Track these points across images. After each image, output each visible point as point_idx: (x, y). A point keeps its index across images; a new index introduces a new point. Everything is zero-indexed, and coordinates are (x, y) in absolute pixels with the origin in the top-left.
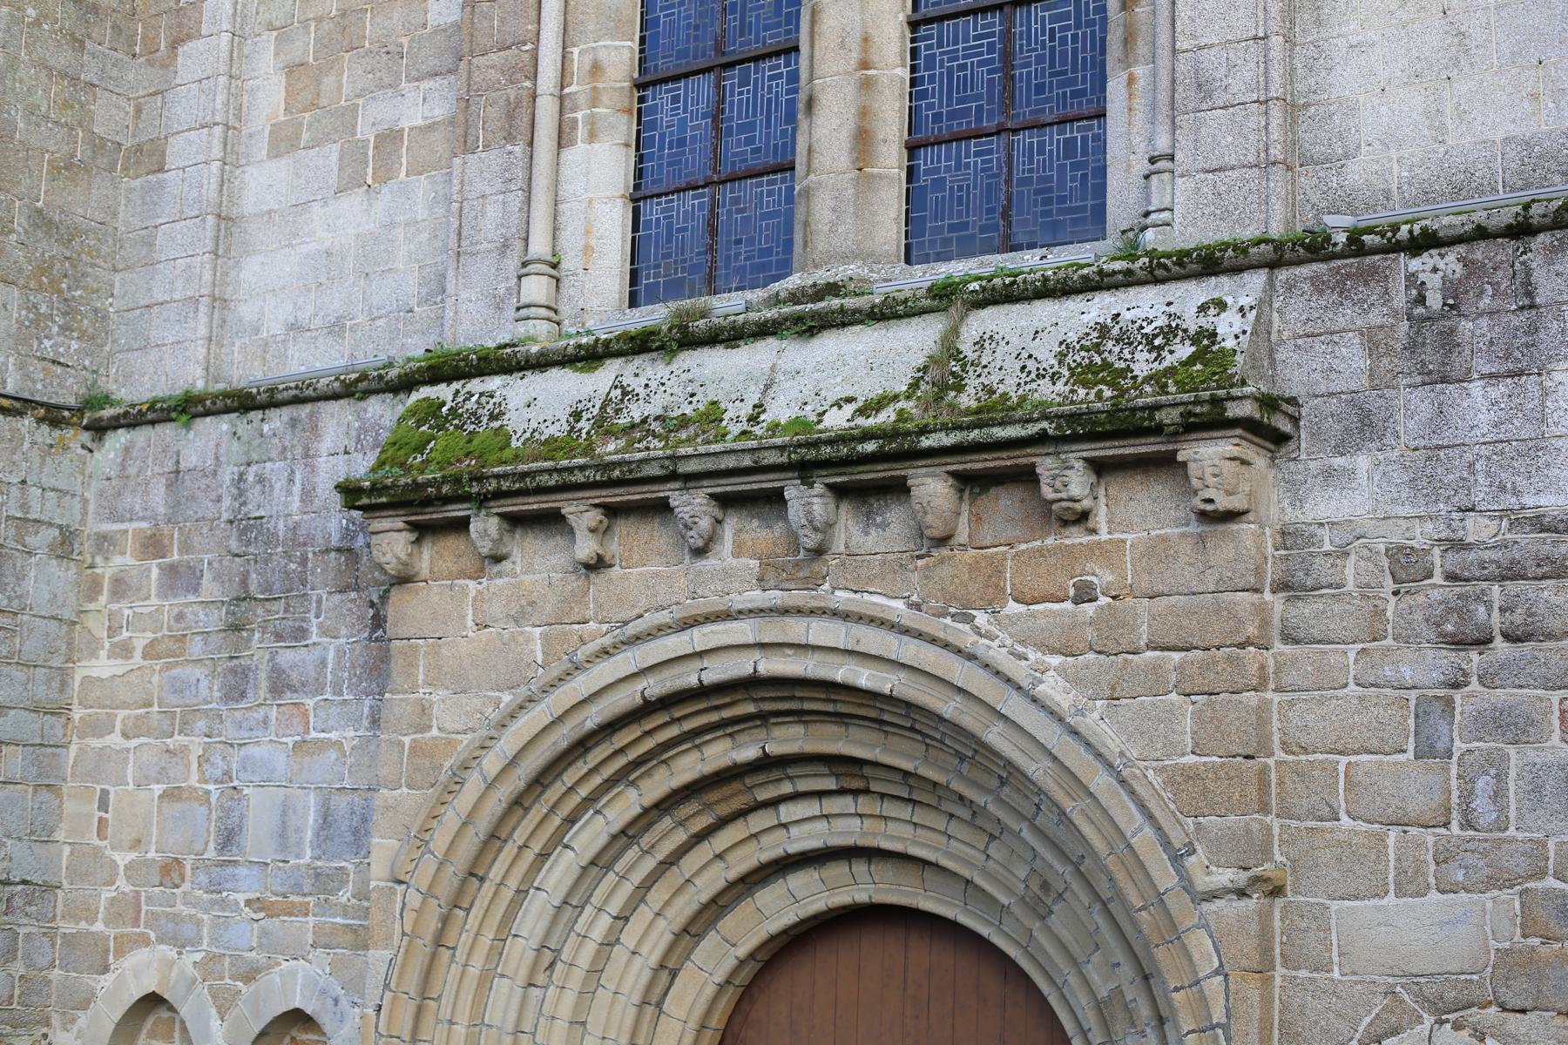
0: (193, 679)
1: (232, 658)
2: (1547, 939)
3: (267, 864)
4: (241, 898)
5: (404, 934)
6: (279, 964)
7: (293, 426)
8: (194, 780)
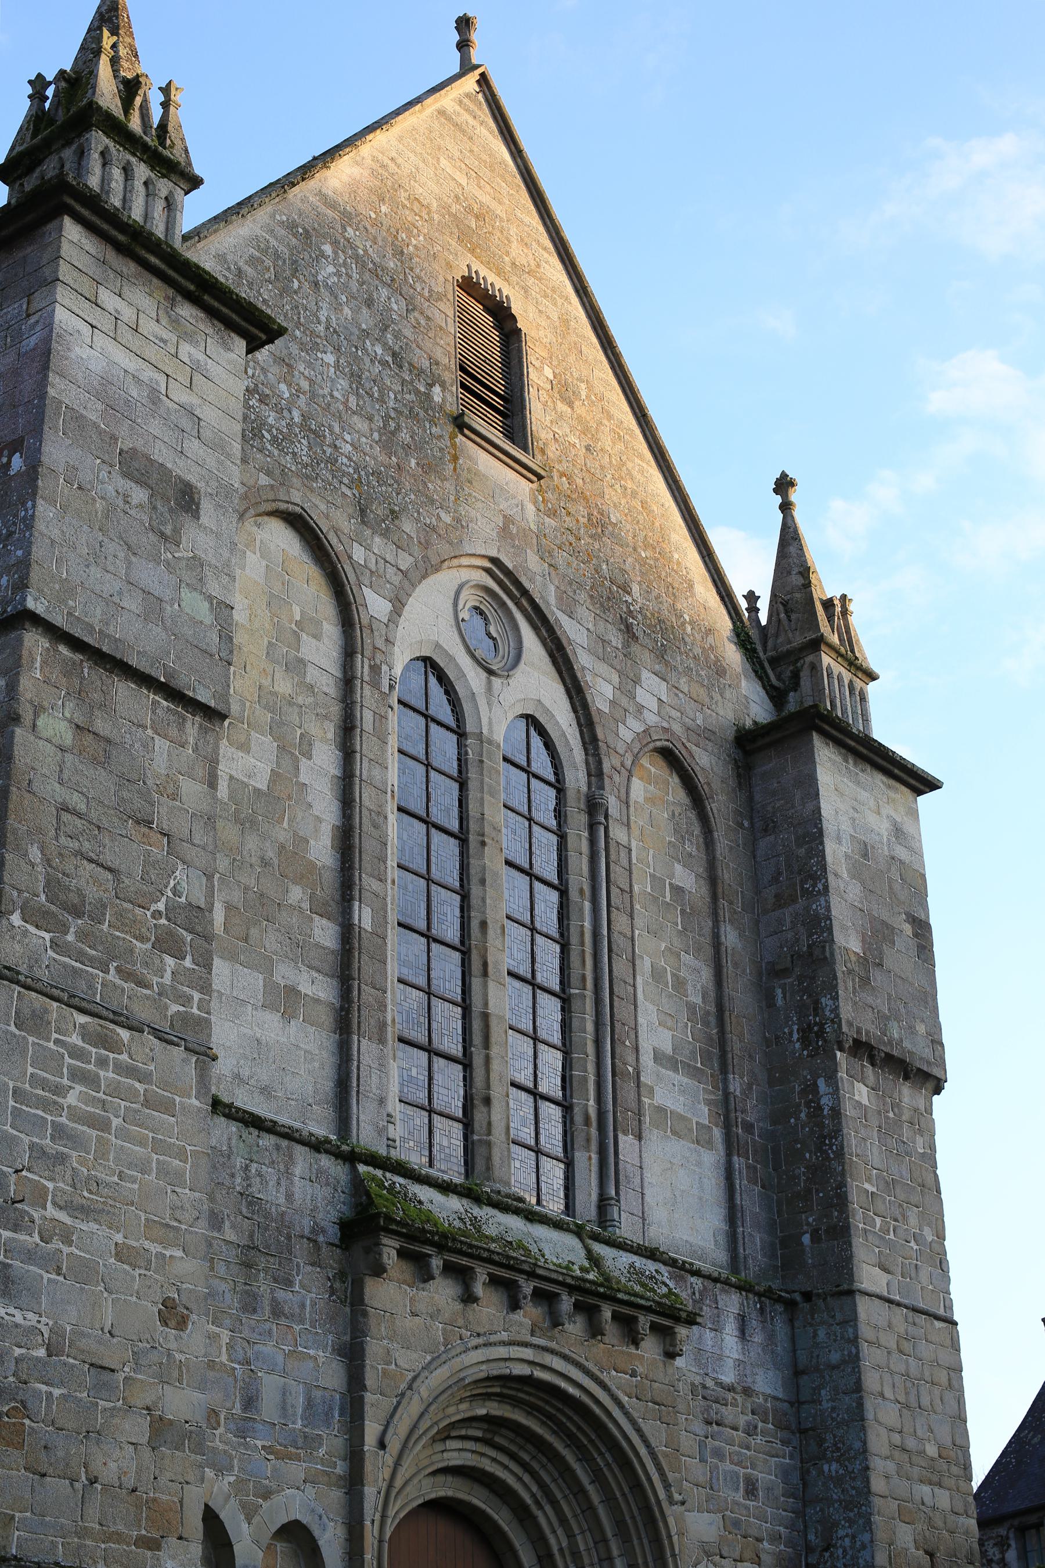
0: (221, 1290)
1: (246, 1284)
2: (730, 1533)
3: (275, 1425)
4: (259, 1443)
5: (384, 1480)
6: (284, 1490)
7: (278, 1150)
8: (224, 1358)
